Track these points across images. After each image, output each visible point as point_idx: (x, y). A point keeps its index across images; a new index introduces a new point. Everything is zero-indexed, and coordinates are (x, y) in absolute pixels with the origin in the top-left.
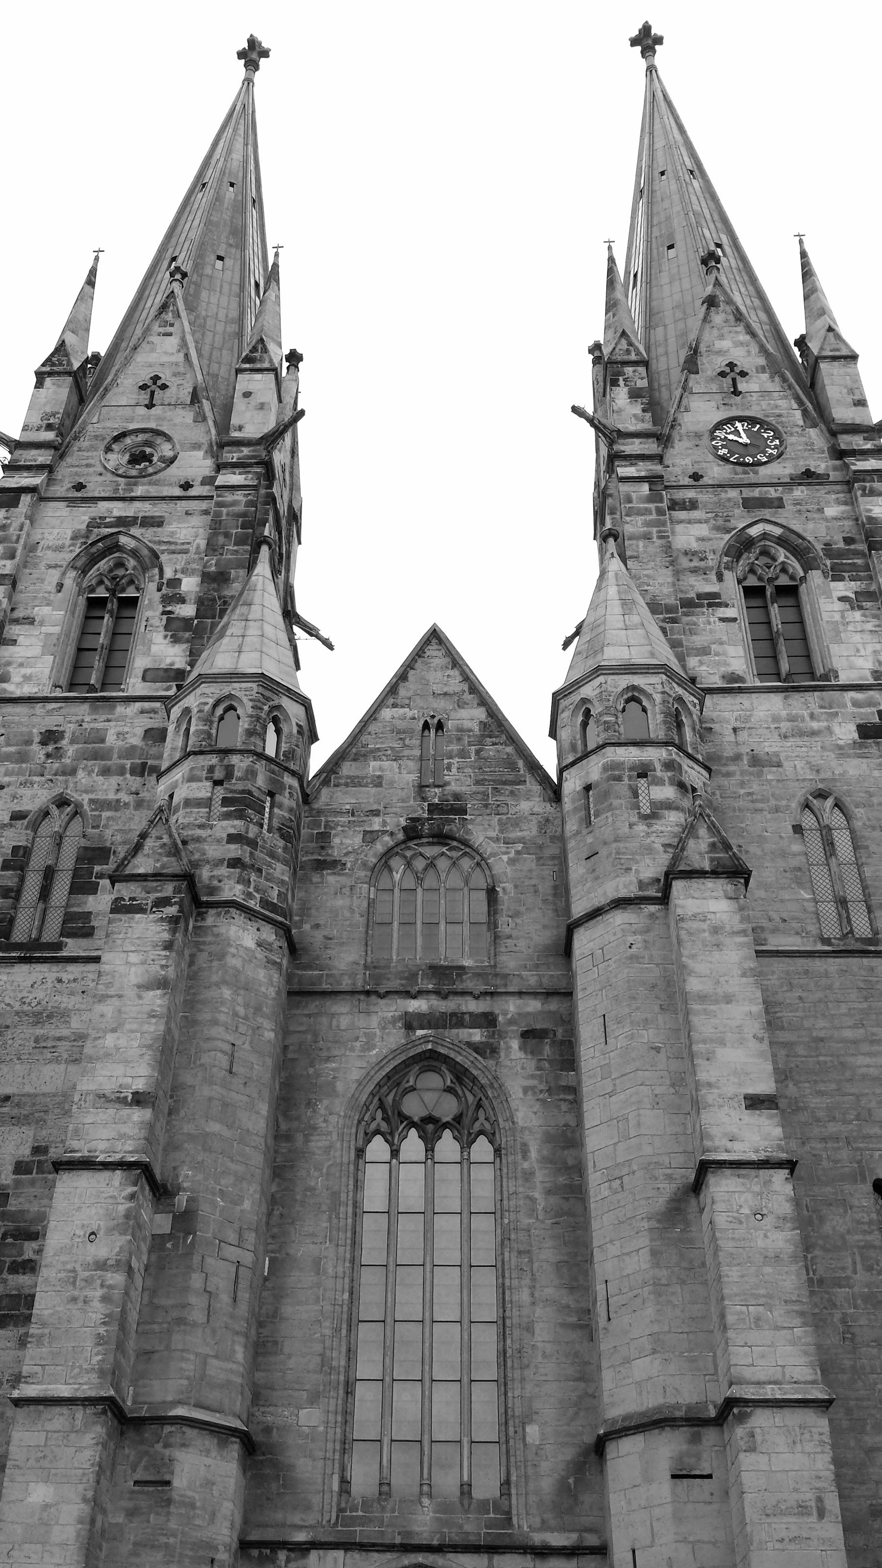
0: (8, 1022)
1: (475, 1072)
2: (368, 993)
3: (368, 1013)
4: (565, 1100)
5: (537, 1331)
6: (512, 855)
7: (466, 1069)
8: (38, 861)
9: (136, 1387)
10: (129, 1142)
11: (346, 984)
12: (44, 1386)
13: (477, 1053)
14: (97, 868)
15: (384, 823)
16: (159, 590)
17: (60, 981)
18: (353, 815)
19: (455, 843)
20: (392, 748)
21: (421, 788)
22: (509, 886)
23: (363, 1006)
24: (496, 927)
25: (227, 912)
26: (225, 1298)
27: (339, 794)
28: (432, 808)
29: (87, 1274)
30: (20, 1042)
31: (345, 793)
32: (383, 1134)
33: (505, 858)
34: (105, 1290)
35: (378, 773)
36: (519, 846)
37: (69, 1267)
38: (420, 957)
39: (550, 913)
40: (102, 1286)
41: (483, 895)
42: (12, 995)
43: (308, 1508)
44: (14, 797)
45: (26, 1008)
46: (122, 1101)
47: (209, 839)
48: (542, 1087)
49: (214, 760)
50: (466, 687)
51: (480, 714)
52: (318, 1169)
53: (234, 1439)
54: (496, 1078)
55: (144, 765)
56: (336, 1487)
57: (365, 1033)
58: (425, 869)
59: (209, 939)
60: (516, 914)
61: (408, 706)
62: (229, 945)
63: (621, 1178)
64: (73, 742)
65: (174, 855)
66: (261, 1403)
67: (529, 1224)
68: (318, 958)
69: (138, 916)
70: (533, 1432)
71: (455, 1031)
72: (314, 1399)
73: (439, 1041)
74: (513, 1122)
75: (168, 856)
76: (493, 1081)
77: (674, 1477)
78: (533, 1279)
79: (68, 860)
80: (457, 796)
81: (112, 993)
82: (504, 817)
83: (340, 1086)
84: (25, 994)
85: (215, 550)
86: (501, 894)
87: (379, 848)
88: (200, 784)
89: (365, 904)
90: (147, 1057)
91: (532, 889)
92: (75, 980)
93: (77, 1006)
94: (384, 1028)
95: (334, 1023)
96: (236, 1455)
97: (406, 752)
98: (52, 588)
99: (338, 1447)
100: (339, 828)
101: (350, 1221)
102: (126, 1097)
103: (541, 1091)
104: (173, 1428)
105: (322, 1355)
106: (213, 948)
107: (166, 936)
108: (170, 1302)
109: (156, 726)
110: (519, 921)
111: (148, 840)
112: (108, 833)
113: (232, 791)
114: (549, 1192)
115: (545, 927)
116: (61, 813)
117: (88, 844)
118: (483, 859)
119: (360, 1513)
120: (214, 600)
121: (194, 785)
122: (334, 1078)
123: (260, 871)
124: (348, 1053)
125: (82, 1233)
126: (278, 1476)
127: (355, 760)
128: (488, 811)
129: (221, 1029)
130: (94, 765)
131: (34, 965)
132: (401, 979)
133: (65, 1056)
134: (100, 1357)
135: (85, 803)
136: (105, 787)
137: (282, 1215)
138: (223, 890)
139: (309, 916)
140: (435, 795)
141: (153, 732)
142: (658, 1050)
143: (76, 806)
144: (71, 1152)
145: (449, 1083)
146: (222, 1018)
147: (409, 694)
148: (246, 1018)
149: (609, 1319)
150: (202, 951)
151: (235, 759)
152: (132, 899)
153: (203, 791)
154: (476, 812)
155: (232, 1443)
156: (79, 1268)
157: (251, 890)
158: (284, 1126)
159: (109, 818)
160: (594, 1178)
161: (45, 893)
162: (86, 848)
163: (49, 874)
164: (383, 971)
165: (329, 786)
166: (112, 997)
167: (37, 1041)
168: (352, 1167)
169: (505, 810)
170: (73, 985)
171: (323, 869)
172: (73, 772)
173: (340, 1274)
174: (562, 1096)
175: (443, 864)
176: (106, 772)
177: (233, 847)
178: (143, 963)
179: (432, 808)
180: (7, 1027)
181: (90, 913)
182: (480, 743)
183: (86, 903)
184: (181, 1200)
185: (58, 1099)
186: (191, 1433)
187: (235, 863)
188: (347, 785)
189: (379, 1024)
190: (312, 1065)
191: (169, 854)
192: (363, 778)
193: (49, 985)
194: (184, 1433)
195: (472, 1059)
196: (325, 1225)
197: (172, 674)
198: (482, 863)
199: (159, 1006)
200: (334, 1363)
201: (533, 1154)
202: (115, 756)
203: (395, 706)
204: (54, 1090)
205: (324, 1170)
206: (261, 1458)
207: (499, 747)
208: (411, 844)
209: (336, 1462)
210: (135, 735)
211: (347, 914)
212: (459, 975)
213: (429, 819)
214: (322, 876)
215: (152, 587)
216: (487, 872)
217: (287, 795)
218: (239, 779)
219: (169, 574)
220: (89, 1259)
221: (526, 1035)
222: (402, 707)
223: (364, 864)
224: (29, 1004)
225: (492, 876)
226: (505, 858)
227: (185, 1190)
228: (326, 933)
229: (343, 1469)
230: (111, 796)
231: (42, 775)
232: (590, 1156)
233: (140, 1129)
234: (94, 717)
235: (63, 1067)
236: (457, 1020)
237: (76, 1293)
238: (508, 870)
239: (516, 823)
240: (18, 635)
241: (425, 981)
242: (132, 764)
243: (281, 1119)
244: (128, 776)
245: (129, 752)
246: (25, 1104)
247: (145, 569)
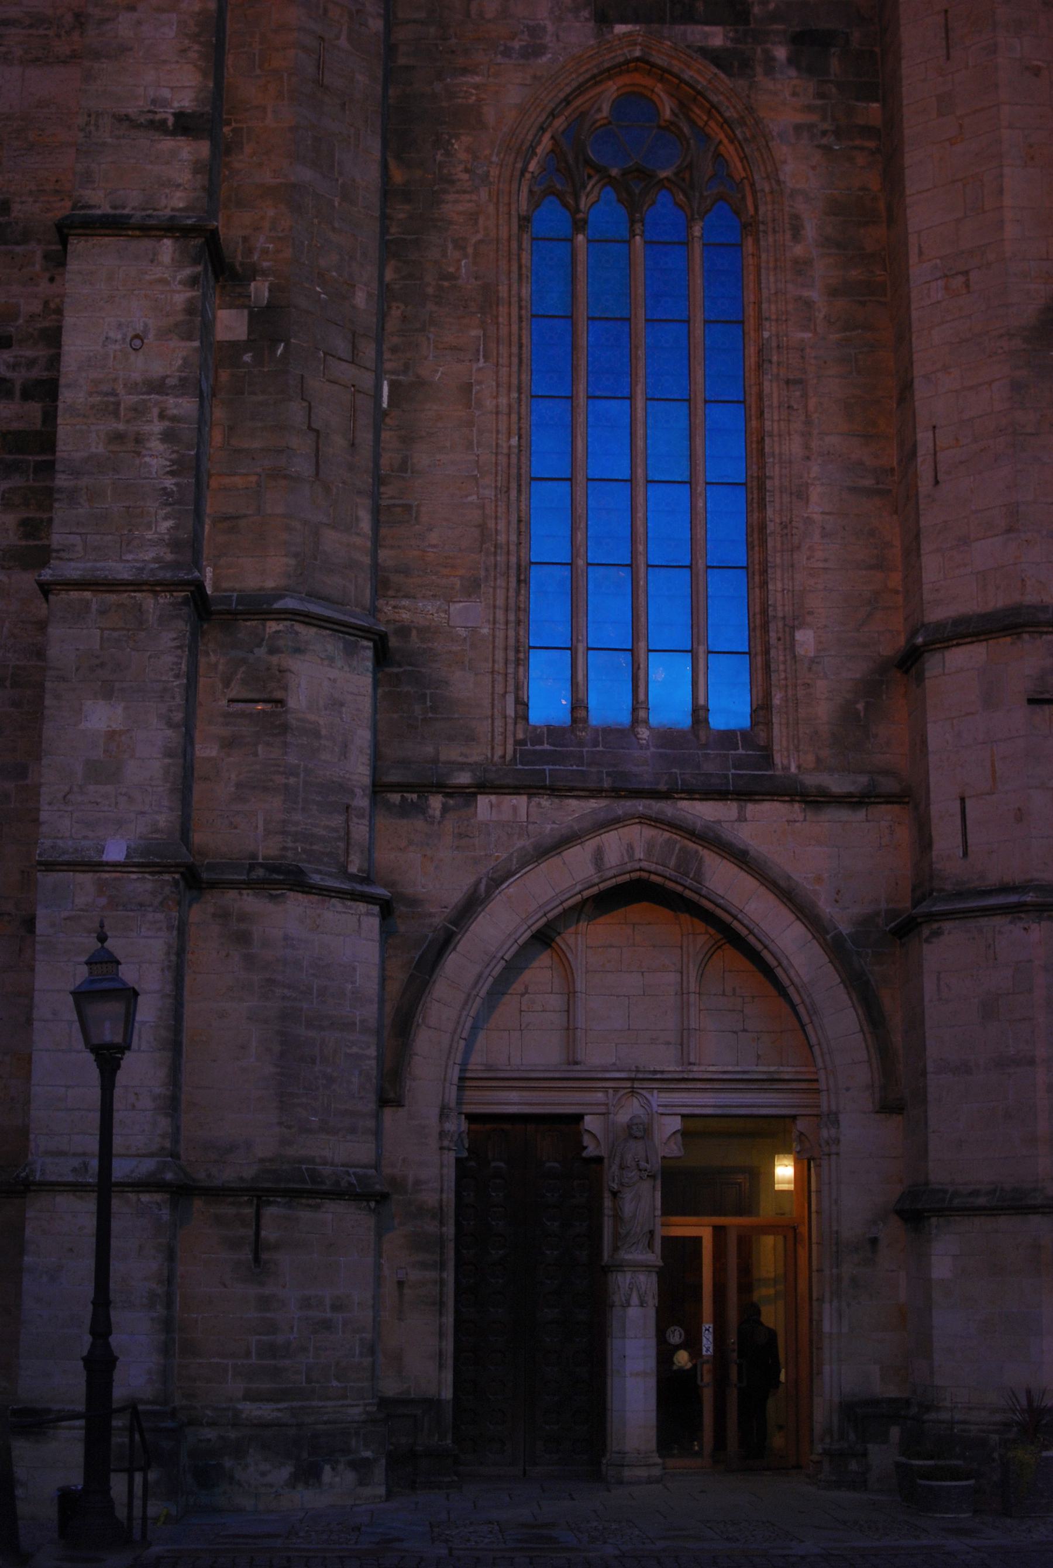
4: (862, 149)
5: (814, 497)
9: (215, 567)
10: (178, 194)
12: (89, 564)
13: (718, 66)
26: (340, 441)
29: (135, 398)
32: (559, 195)
34: (167, 423)
37: (105, 388)
40: (162, 416)
43: (471, 738)
46: (158, 126)
48: (826, 126)
52: (460, 245)
53: (366, 643)
54: (750, 109)
56: (511, 712)
63: (966, 273)
66: (391, 593)
67: (802, 340)
70: (806, 639)
71: (679, 29)
72: (472, 587)
74: (778, 182)
77: (1031, 701)
78: (808, 422)
83: (490, 115)
90: (192, 55)
96: (369, 664)
99: (512, 656)
101: (515, 328)
102: (164, 121)
103: (824, 133)
104: (281, 626)
105: (482, 527)
108: (256, 445)
114: (833, 292)
119: (546, 747)
124: (499, 59)
125: (119, 337)
126: (424, 695)
134: (170, 523)
137: (404, 319)
142: (1037, 72)
144: (83, 207)
149: (937, 482)
155: (366, 648)
156: (120, 389)
158: (398, 176)
160: (918, 271)
168: (514, 245)
173: (504, 409)
174: (857, 142)
184: (260, 290)
186: (307, 632)
194: (297, 633)
196: (474, 333)
200: (502, 539)
201: (810, 231)
205: (470, 250)
206: (396, 670)
209: (511, 676)
220: (136, 376)
221: (799, 40)
227: (265, 273)
229: (518, 687)
232: (913, 239)
233: (196, 172)
237: (121, 427)
243: (392, 164)
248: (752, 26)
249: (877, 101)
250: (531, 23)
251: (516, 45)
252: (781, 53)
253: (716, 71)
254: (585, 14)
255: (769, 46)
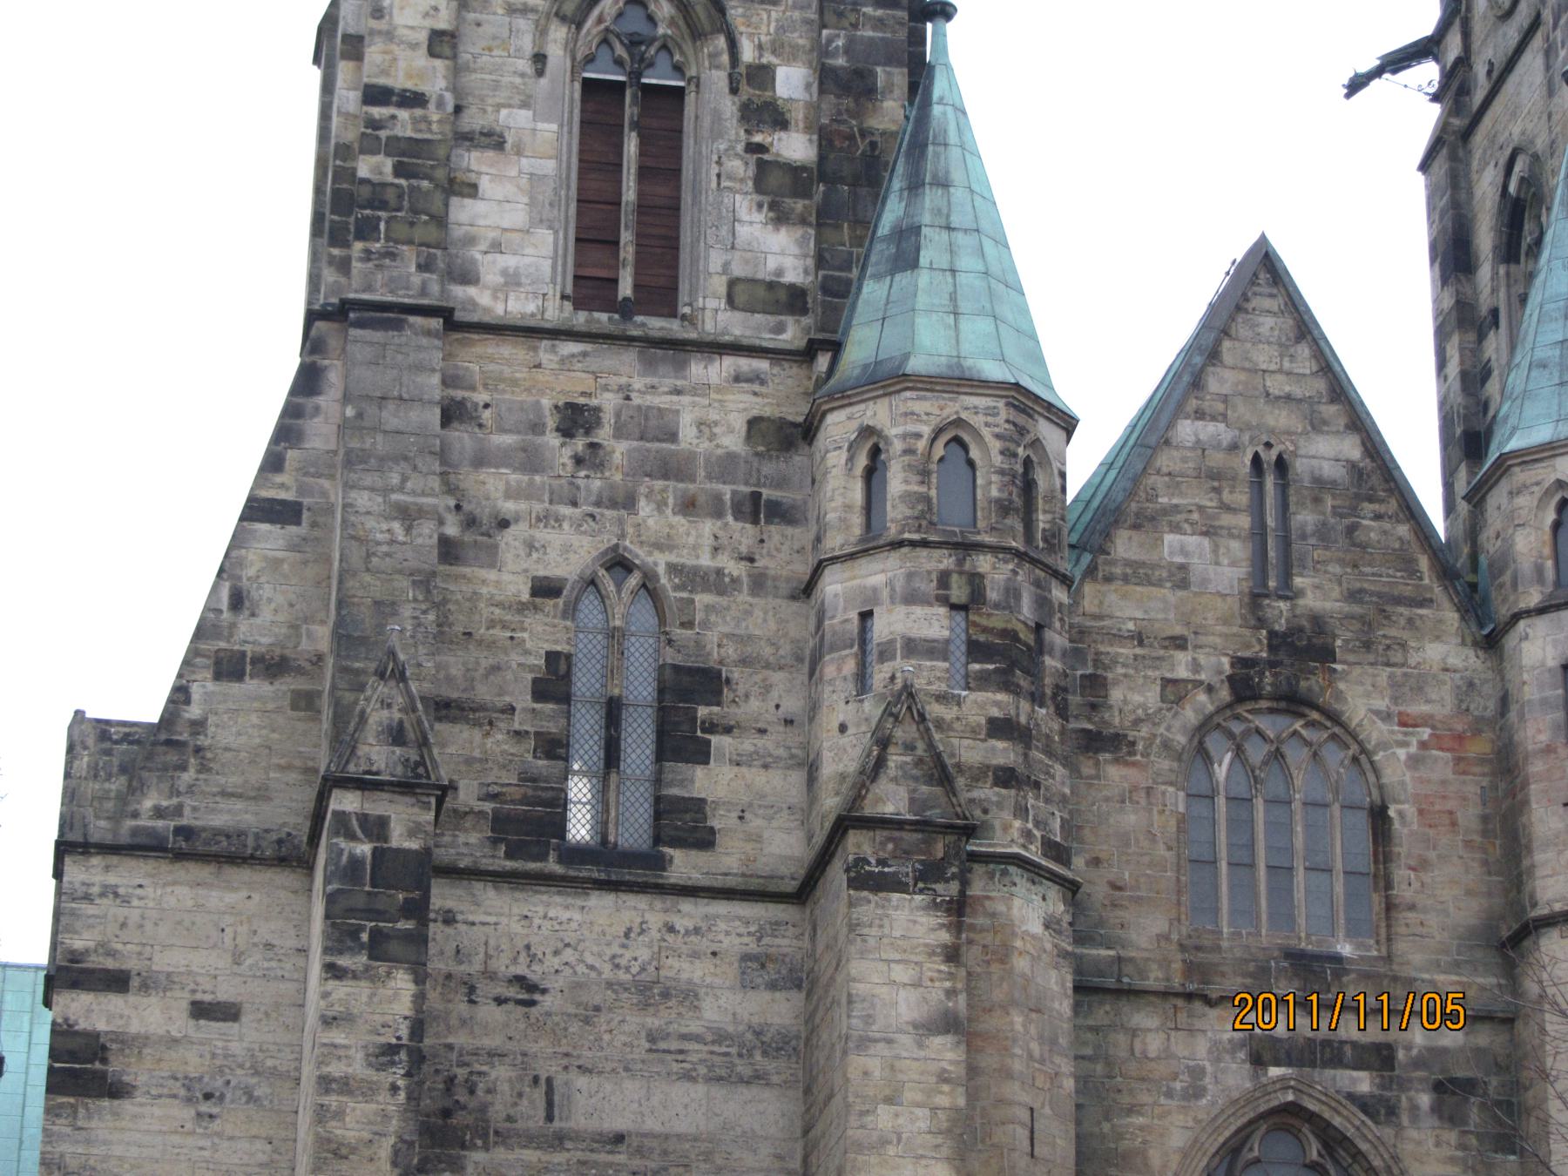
0: (597, 1000)
1: (1364, 1147)
2: (1189, 997)
3: (1191, 1031)
6: (1413, 749)
7: (1346, 1138)
8: (585, 682)
11: (1154, 979)
13: (1366, 1113)
14: (703, 711)
15: (1196, 666)
16: (734, 91)
17: (671, 929)
18: (1141, 644)
19: (1315, 715)
20: (1201, 508)
21: (1255, 599)
22: (1410, 809)
23: (1182, 1018)
24: (1389, 885)
25: (1005, 873)
27: (1113, 597)
28: (1277, 641)
30: (623, 1038)
31: (1124, 597)
33: (1402, 753)
35: (1179, 559)
36: (1425, 733)
38: (1268, 937)
39: (1476, 867)
41: (1361, 821)
42: (595, 949)
44: (531, 546)
45: (623, 976)
47: (957, 725)
49: (945, 560)
50: (1320, 385)
51: (1351, 448)
54: (1396, 1159)
55: (756, 496)
57: (1188, 1067)
58: (1265, 763)
59: (980, 921)
60: (1422, 865)
61: (1224, 417)
62: (1014, 934)
64: (619, 433)
65: (941, 783)
68: (1101, 923)
69: (896, 896)
73: (1305, 1089)
75: (926, 783)
76: (1391, 1163)
79: (640, 687)
80: (1317, 620)
81: (878, 1035)
82: (1398, 671)
84: (616, 949)
85: (840, 15)
86: (1397, 825)
87: (1190, 715)
88: (928, 610)
89: (1173, 822)
91: (1446, 820)
92: (697, 931)
93: (708, 980)
94: (1219, 1060)
95: (1138, 1047)
97: (1226, 519)
98: (525, 65)
100: (1120, 670)
106: (988, 938)
107: (945, 937)
109: (768, 412)
110: (1427, 877)
111: (891, 749)
112: (712, 637)
113: (985, 630)
115: (1469, 893)
116: (619, 586)
117: (679, 660)
118: (1363, 750)
120: (851, 137)
121: (919, 611)
122: (1144, 1142)
123: (1037, 785)
124: (1162, 1100)
127: (1136, 527)
128: (1371, 658)
129: (1016, 1086)
130: (665, 490)
131: (624, 896)
132: (1245, 975)
133: (702, 1070)
135: (661, 570)
136: (691, 540)
138: (992, 827)
139: (1081, 841)
140: (1280, 612)
141: (763, 426)
143: (645, 575)
145: (1314, 1155)
146: (1017, 1066)
147: (1226, 389)
148: (1042, 1061)
150: (970, 942)
151: (984, 563)
152: (882, 862)
153: (936, 624)
154: (1351, 658)
157: (1030, 825)
159: (709, 608)
161: (612, 755)
162: (676, 668)
163: (613, 711)
164: (1213, 958)
165: (1095, 580)
166: (876, 1041)
167: (652, 1038)
169: (1397, 657)
170: (693, 938)
171: (1097, 751)
172: (628, 503)
175: (1296, 755)
176: (688, 506)
177: (1000, 745)
178: (917, 985)
179: (1277, 641)
180: (597, 1009)
181: (703, 801)
182: (1354, 510)
183: (692, 781)
185: (704, 1146)
187: (1006, 777)
188: (1126, 579)
189: (1210, 1052)
190: (1107, 1119)
191: (930, 780)
192: (1154, 567)
193: (655, 935)
195: (1358, 1123)
197: (783, 296)
198: (1362, 759)
199: (951, 1062)
202: (702, 473)
203: (1200, 415)
204: (693, 1130)
207: (1387, 526)
208: (1241, 710)
210: (731, 431)
211: (1145, 844)
212: (1338, 975)
213: (1272, 664)
214: (1097, 763)
215: (717, 79)
216: (1372, 778)
217: (1057, 625)
218: (997, 606)
219: (748, 54)
222: (1213, 418)
223: (1166, 745)
224: (628, 969)
225: (1381, 787)
226: (1402, 753)
228: (1111, 877)
230: (705, 561)
231: (575, 504)
234: (649, 380)
235: (699, 1090)
236: (1330, 1054)
238: (1408, 778)
239: (1418, 684)
240: (479, 173)
241: (1283, 983)
242: (734, 493)
244: (730, 519)
245: (725, 466)
246: (651, 1150)
247: (697, 35)
248: (1397, 1072)
249: (1514, 1153)
250: (1191, 1063)
251: (1178, 1085)
252: (1425, 1100)
253: (1364, 1118)
254: (1242, 1055)
255: (1412, 1093)
